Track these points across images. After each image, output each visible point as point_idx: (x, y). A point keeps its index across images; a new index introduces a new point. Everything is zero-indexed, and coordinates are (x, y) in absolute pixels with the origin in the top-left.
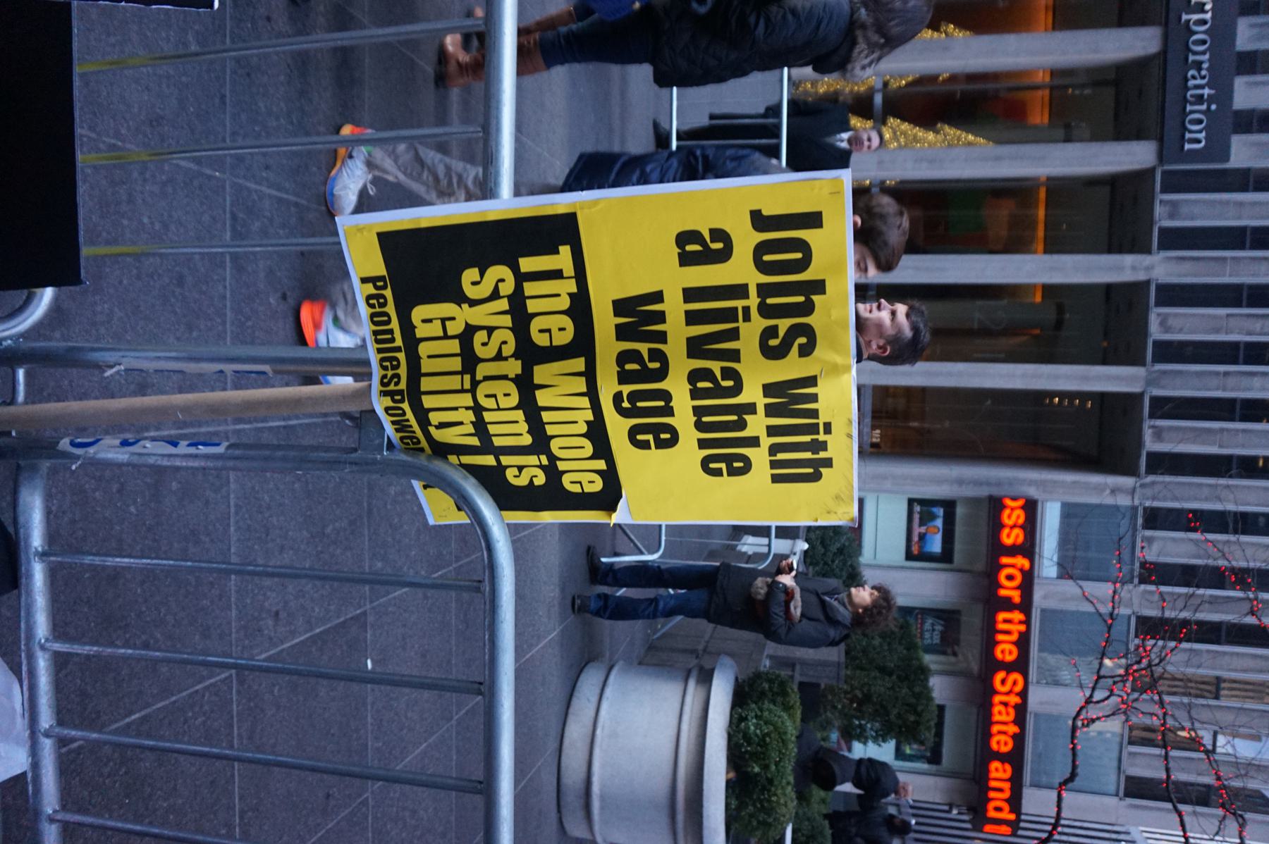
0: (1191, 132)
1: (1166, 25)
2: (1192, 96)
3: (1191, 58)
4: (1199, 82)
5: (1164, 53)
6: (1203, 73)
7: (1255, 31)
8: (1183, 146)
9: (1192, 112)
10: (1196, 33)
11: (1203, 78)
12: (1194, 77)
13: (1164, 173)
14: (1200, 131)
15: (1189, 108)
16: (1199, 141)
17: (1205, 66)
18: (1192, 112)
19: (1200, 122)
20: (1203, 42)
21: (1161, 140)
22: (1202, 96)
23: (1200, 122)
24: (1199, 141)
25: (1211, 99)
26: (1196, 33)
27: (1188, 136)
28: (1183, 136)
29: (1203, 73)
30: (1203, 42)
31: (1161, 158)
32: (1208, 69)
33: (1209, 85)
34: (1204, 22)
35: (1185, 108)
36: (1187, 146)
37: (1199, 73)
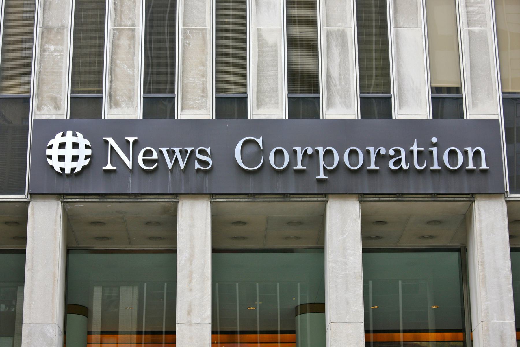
0: (466, 162)
1: (325, 195)
2: (420, 164)
3: (373, 166)
4: (403, 156)
5: (362, 197)
6: (392, 152)
7: (337, 100)
8: (484, 171)
9: (441, 162)
10: (341, 161)
11: (398, 152)
12: (398, 162)
13: (512, 191)
14: (466, 153)
15: (436, 167)
16: (477, 154)
17: (383, 151)
18: (441, 162)
19: (453, 153)
20: (353, 153)
21: (472, 196)
22: (419, 152)
23: (453, 153)
24: (477, 154)
25: (424, 142)
26: (341, 161)
27: (471, 166)
28: (471, 171)
29: (392, 152)
30: (353, 153)
31: (498, 193)
32: (387, 150)
33: (407, 145)
34: (328, 153)
35: (434, 171)
36: (484, 166)
37: (392, 157)
